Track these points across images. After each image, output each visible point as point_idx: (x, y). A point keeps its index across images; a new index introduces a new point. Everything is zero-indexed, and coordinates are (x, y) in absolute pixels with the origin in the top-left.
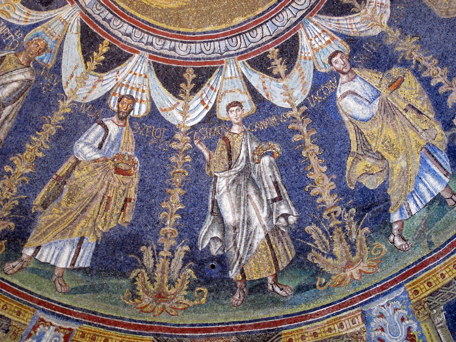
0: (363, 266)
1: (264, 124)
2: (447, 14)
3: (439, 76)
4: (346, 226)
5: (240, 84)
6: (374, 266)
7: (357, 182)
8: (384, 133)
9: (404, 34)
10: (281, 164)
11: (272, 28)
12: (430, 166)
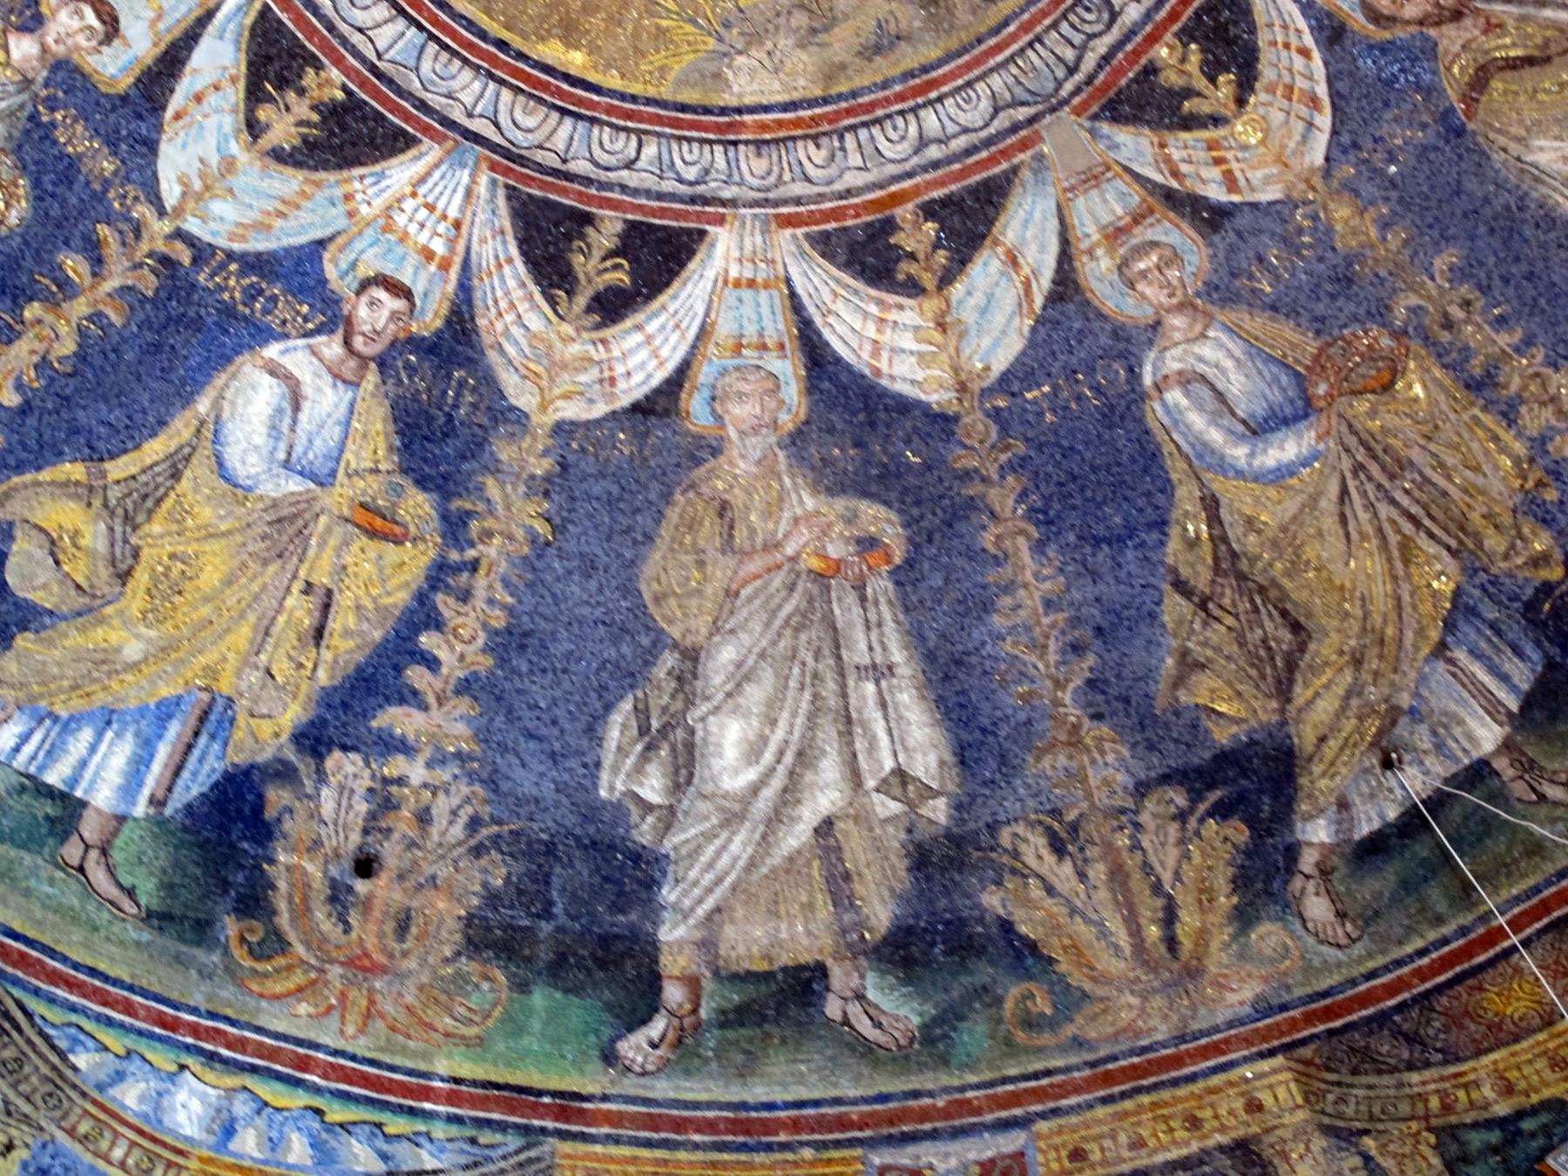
2: (657, 600)
3: (458, 647)
7: (11, 524)
8: (208, 546)
9: (544, 488)
11: (404, 50)
12: (160, 737)
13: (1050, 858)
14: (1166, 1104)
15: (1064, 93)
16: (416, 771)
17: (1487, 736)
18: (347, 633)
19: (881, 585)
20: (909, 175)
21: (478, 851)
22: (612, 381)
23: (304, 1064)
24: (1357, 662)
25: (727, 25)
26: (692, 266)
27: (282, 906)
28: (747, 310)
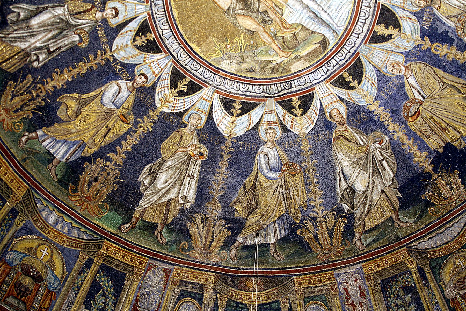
0: (8, 121)
1: (101, 33)
4: (33, 102)
5: (131, 15)
6: (8, 128)
10: (73, 49)
13: (200, 222)
14: (195, 273)
15: (275, 95)
17: (273, 240)
18: (110, 137)
19: (199, 162)
20: (242, 95)
21: (115, 183)
22: (174, 107)
23: (73, 214)
24: (262, 216)
25: (226, 54)
26: (198, 92)
27: (80, 184)
28: (203, 104)
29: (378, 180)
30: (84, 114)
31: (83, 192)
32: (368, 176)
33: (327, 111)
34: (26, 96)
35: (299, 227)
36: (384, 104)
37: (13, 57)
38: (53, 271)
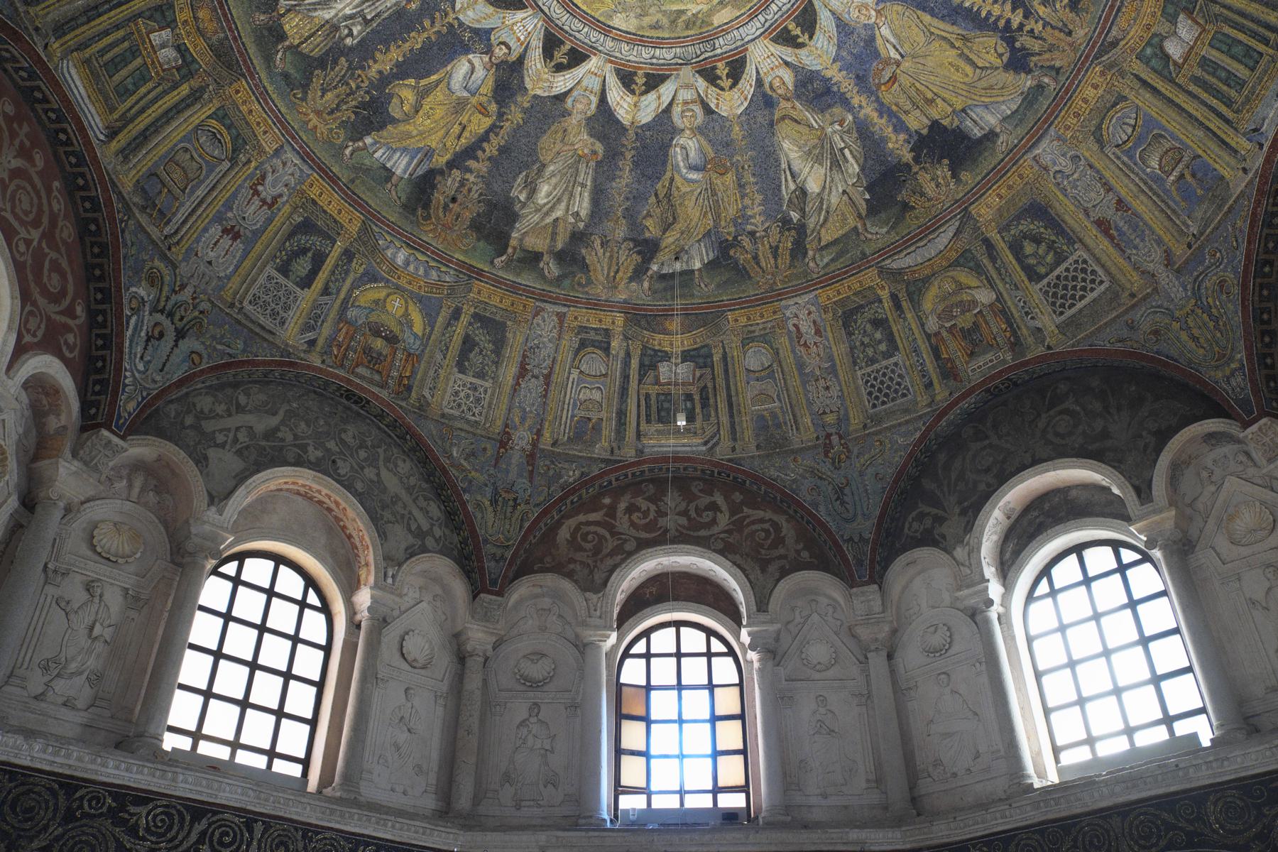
3: (491, 149)
16: (472, 178)
17: (698, 265)
19: (592, 164)
23: (428, 249)
24: (682, 233)
29: (838, 177)
30: (426, 107)
31: (438, 218)
32: (823, 171)
33: (767, 80)
34: (342, 89)
35: (732, 246)
36: (846, 67)
37: (314, 33)
38: (411, 327)
